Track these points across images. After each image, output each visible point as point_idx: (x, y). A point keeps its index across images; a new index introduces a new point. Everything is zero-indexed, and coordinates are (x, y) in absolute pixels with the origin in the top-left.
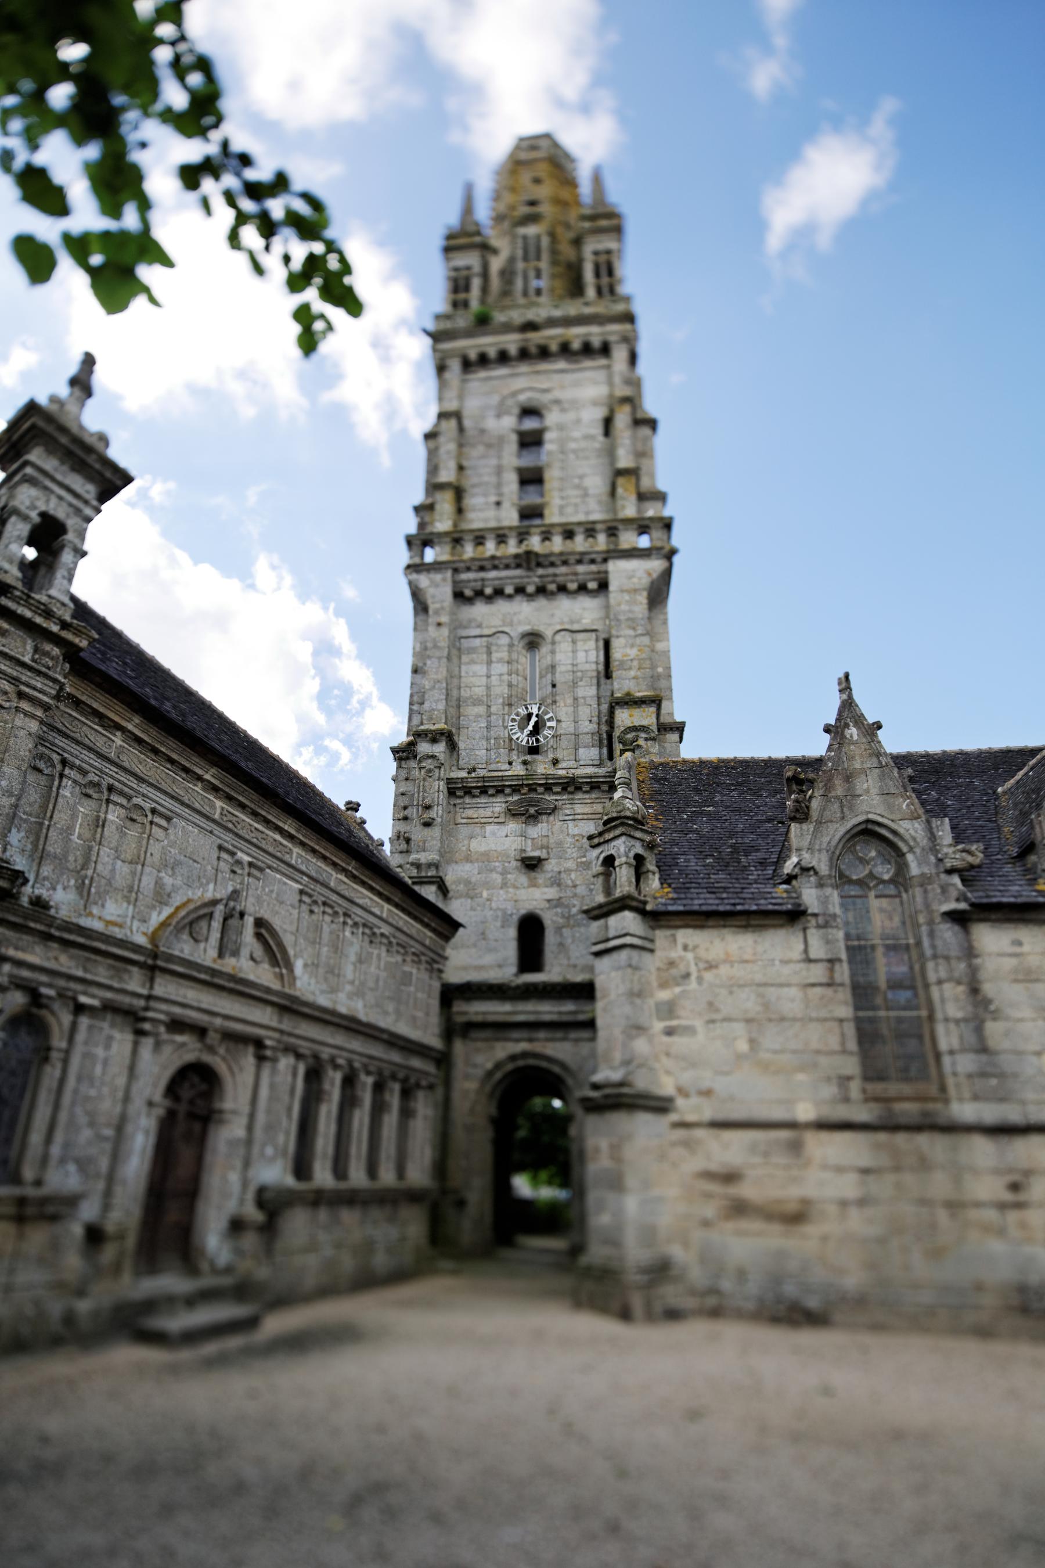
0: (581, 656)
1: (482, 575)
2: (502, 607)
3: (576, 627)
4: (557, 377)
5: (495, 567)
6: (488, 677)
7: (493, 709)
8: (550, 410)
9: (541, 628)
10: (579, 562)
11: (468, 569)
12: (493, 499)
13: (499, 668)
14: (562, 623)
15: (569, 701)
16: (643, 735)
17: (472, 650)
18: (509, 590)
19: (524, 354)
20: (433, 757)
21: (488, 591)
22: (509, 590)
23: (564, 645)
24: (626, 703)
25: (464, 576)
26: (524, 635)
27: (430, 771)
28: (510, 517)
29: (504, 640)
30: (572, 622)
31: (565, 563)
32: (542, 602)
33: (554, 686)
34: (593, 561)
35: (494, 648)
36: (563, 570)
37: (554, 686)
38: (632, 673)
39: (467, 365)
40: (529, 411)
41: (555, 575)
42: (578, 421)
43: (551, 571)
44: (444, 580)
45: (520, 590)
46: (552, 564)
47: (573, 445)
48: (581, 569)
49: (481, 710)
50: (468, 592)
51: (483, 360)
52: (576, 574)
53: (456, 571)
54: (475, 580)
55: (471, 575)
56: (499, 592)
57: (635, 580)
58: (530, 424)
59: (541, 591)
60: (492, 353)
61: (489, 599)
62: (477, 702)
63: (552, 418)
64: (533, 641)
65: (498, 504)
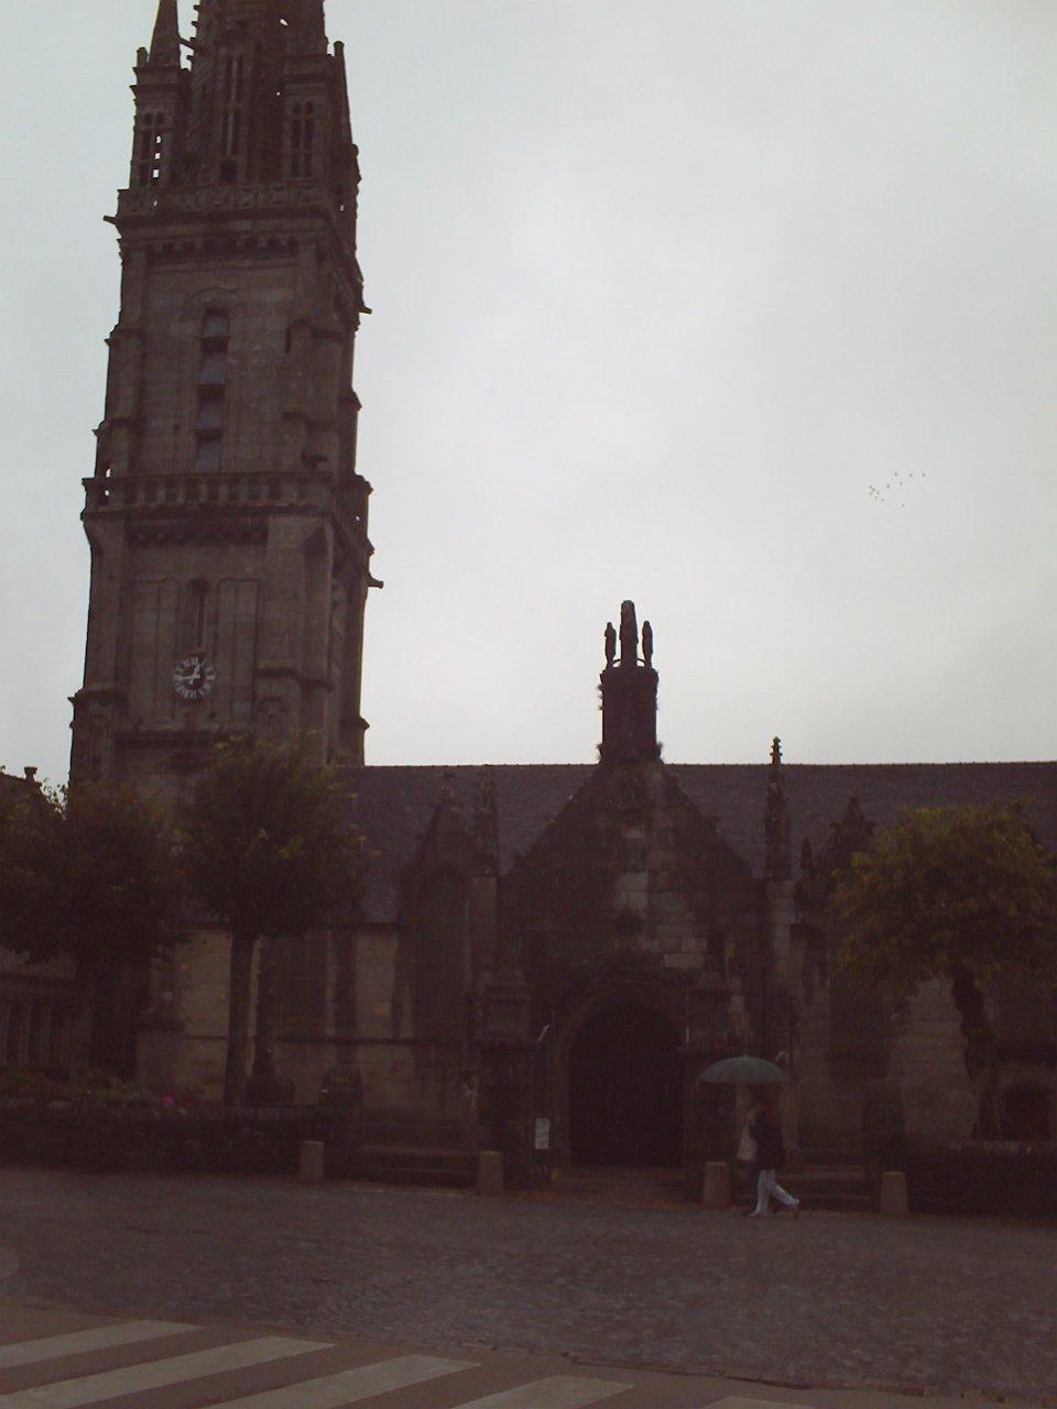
21: (160, 536)
40: (213, 312)
47: (254, 361)
58: (215, 328)
65: (177, 428)
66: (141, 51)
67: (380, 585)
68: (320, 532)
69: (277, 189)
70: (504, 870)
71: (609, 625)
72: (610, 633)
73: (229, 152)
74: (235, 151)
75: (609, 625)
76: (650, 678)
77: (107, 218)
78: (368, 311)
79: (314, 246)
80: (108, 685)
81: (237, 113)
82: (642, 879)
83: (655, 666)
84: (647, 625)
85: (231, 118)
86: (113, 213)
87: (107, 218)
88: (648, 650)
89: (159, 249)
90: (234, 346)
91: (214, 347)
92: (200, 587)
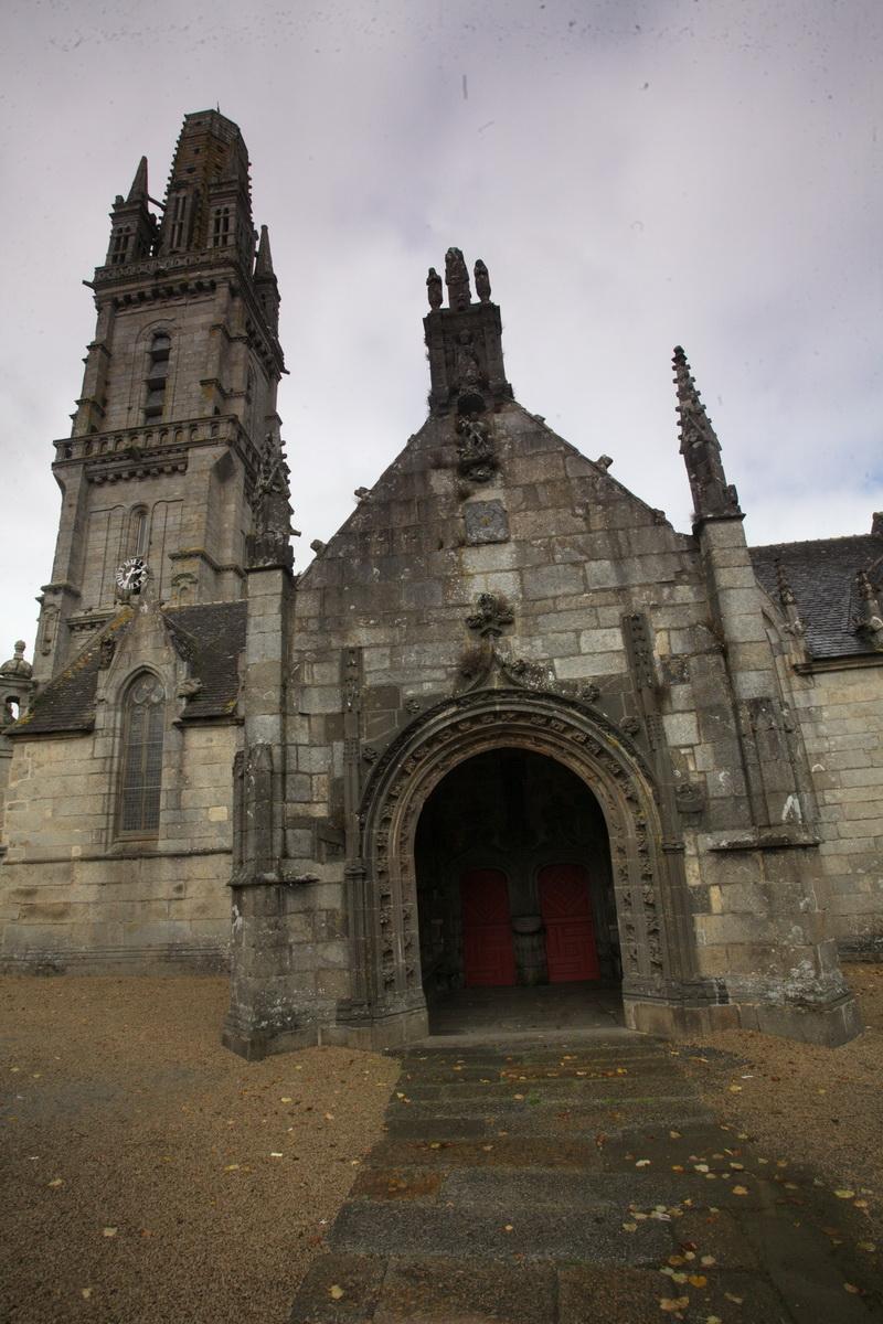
0: (171, 519)
1: (105, 466)
2: (122, 486)
3: (170, 498)
4: (178, 309)
5: (113, 460)
6: (107, 540)
7: (108, 564)
8: (174, 335)
9: (146, 502)
10: (169, 452)
11: (95, 463)
12: (127, 405)
13: (115, 534)
14: (161, 497)
15: (160, 555)
16: (190, 580)
17: (98, 522)
18: (125, 475)
19: (156, 295)
20: (53, 605)
21: (111, 477)
22: (125, 475)
23: (160, 512)
24: (179, 557)
25: (92, 468)
26: (135, 507)
27: (51, 615)
28: (137, 419)
29: (120, 512)
30: (167, 495)
31: (159, 453)
32: (149, 481)
33: (151, 543)
34: (179, 451)
35: (113, 518)
36: (160, 458)
37: (151, 543)
38: (192, 533)
39: (117, 305)
40: (160, 336)
41: (155, 462)
42: (193, 341)
43: (152, 459)
44: (77, 472)
45: (132, 474)
46: (151, 455)
47: (186, 361)
48: (171, 456)
49: (101, 565)
50: (97, 479)
51: (128, 301)
52: (169, 460)
53: (86, 464)
54: (101, 470)
55: (97, 467)
56: (118, 477)
57: (205, 463)
58: (161, 345)
59: (147, 473)
60: (134, 296)
61: (113, 482)
62: (97, 559)
63: (175, 340)
64: (141, 511)
65: (130, 409)
66: (119, 198)
67: (299, 534)
68: (227, 456)
69: (203, 255)
70: (299, 567)
71: (432, 271)
72: (433, 281)
73: (175, 246)
74: (179, 245)
75: (432, 271)
76: (489, 317)
77: (85, 283)
78: (288, 373)
79: (227, 284)
80: (64, 581)
81: (181, 225)
82: (506, 555)
83: (493, 299)
84: (479, 264)
85: (177, 228)
86: (91, 279)
87: (85, 283)
88: (484, 289)
89: (121, 299)
90: (172, 354)
91: (159, 357)
92: (141, 511)
